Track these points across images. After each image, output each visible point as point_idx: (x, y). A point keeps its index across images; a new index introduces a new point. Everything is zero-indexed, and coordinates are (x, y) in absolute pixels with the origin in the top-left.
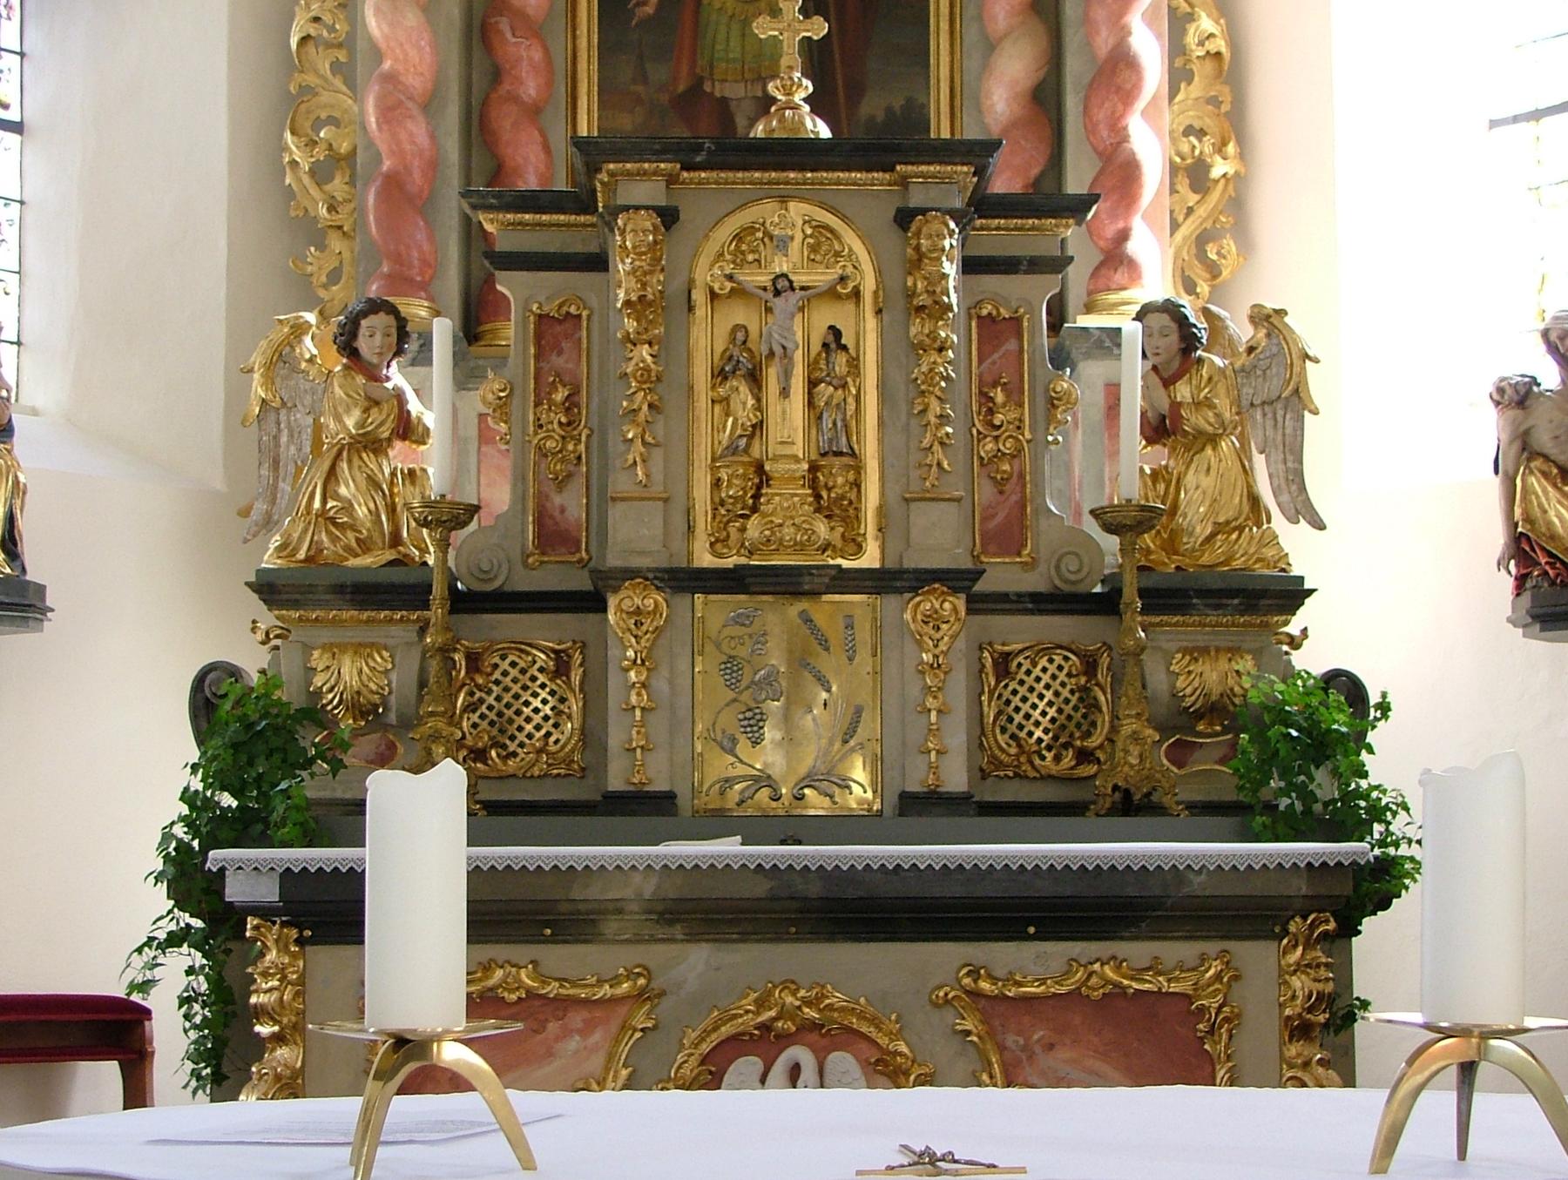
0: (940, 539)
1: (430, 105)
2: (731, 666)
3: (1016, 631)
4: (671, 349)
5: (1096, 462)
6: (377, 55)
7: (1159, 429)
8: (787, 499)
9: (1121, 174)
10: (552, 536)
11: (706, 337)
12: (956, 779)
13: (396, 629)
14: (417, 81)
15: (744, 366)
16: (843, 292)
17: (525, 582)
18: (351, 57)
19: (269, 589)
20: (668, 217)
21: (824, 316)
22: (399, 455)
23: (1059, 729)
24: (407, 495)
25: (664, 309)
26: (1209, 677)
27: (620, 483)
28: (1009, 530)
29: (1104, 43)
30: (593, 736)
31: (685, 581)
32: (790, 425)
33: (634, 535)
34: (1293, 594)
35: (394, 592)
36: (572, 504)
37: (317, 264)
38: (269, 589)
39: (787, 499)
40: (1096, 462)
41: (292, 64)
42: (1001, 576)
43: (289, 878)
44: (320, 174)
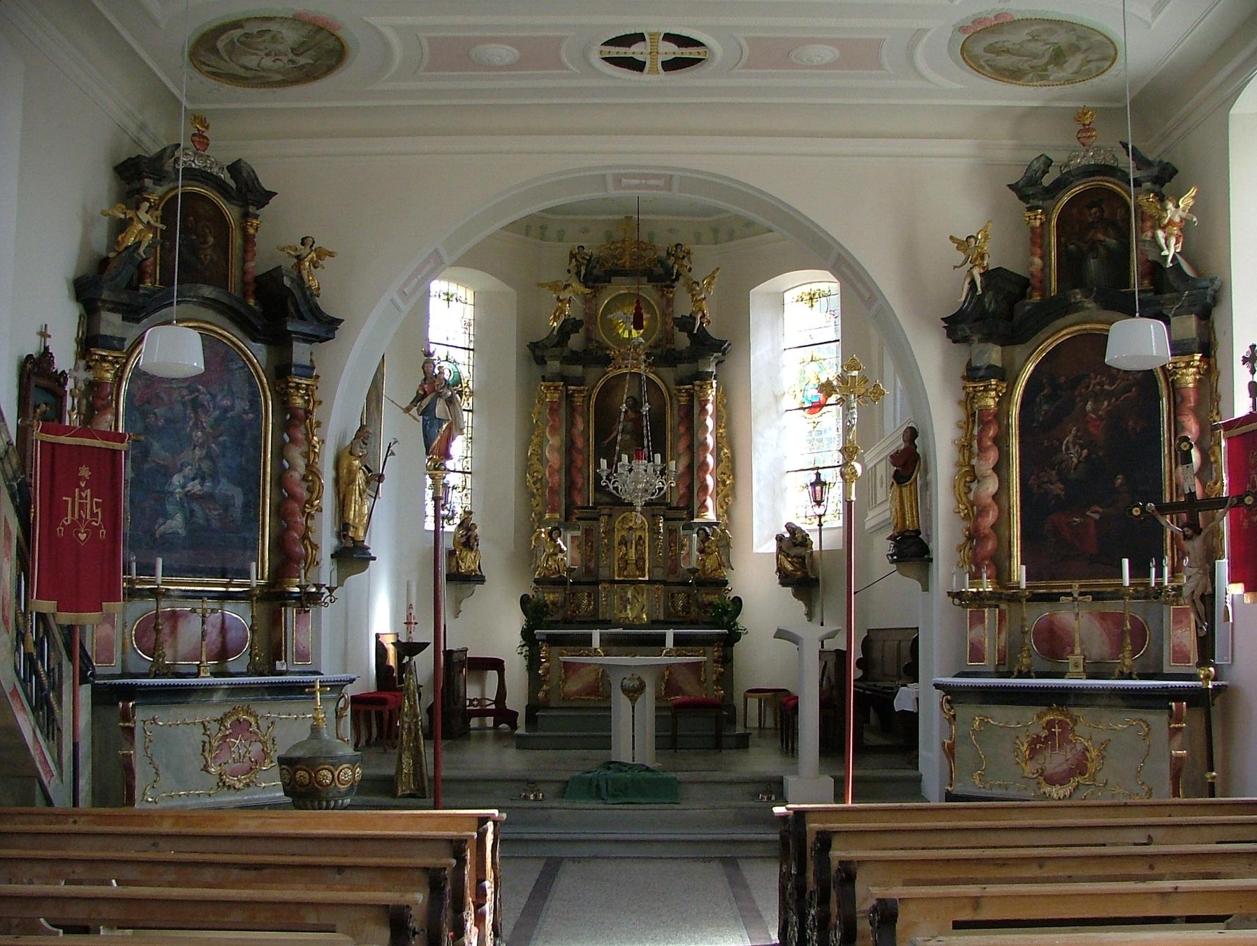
0: (659, 574)
1: (559, 471)
2: (621, 597)
3: (675, 589)
4: (611, 540)
5: (691, 555)
6: (548, 461)
7: (702, 551)
8: (631, 568)
9: (705, 487)
10: (588, 571)
11: (617, 538)
12: (662, 618)
13: (561, 589)
14: (556, 467)
15: (624, 542)
16: (642, 528)
17: (585, 580)
18: (542, 459)
19: (536, 581)
20: (610, 516)
21: (639, 533)
22: (560, 556)
23: (683, 607)
24: (561, 564)
25: (610, 532)
26: (710, 598)
27: (602, 564)
28: (674, 568)
29: (701, 459)
30: (596, 609)
31: (613, 582)
32: (632, 554)
33: (604, 573)
34: (726, 583)
35: (560, 582)
36: (592, 565)
37: (534, 503)
38: (536, 581)
39: (631, 568)
40: (691, 555)
41: (528, 459)
42: (672, 579)
43: (547, 635)
44: (535, 483)
